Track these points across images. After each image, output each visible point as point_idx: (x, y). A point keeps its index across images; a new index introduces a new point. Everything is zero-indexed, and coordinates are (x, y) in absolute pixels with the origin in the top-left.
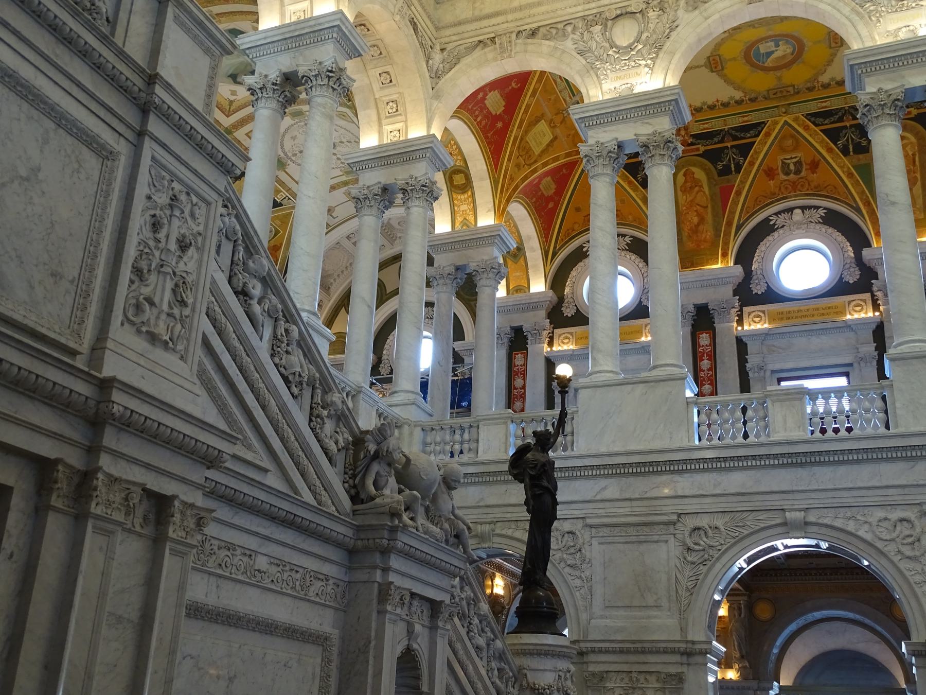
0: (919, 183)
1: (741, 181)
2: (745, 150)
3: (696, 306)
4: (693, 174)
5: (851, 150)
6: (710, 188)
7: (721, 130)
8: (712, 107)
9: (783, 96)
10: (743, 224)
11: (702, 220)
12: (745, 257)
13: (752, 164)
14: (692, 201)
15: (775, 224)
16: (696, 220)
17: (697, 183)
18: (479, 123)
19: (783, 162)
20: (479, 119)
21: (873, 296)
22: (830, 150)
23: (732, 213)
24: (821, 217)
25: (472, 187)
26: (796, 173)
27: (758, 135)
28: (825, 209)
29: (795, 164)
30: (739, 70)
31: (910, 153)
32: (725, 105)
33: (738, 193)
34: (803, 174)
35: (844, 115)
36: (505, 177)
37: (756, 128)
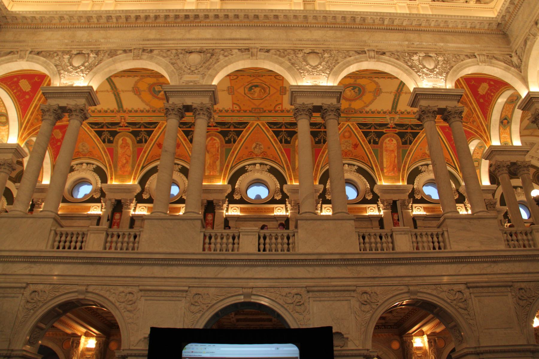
0: (219, 160)
2: (149, 133)
7: (140, 123)
8: (136, 111)
13: (152, 140)
16: (125, 161)
17: (127, 144)
18: (15, 93)
20: (15, 91)
22: (185, 140)
23: (141, 161)
25: (9, 124)
27: (155, 128)
30: (148, 96)
32: (142, 111)
33: (145, 152)
35: (191, 125)
36: (28, 123)
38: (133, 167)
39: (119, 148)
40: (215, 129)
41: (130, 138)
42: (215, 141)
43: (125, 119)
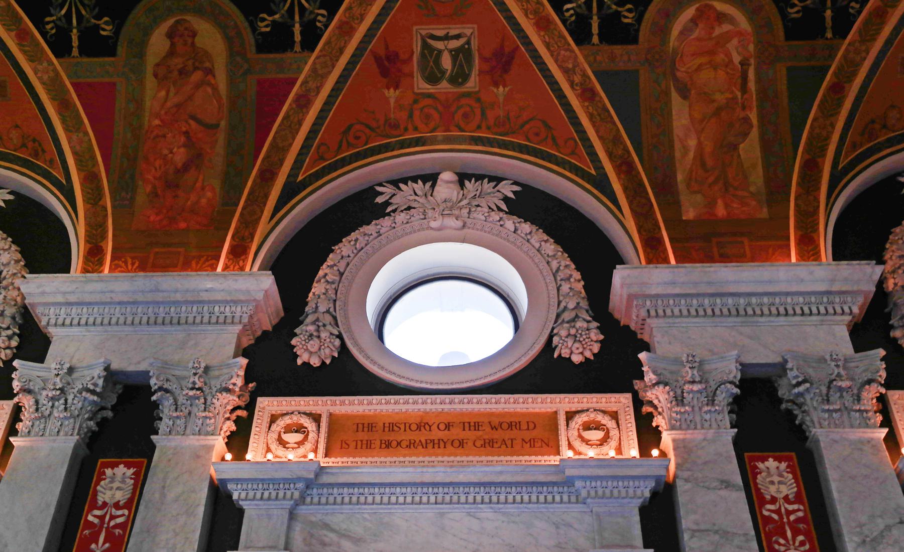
0: (755, 133)
1: (314, 70)
3: (111, 375)
4: (194, 35)
5: (595, 29)
6: (231, 82)
10: (304, 185)
11: (196, 160)
12: (295, 270)
13: (347, 30)
14: (178, 106)
15: (387, 203)
16: (180, 156)
17: (200, 61)
19: (425, 45)
21: (638, 403)
22: (543, 24)
23: (279, 150)
24: (506, 199)
26: (453, 80)
28: (516, 183)
29: (455, 54)
31: (737, 59)
33: (304, 102)
34: (472, 84)
39: (150, 82)
42: (726, 27)
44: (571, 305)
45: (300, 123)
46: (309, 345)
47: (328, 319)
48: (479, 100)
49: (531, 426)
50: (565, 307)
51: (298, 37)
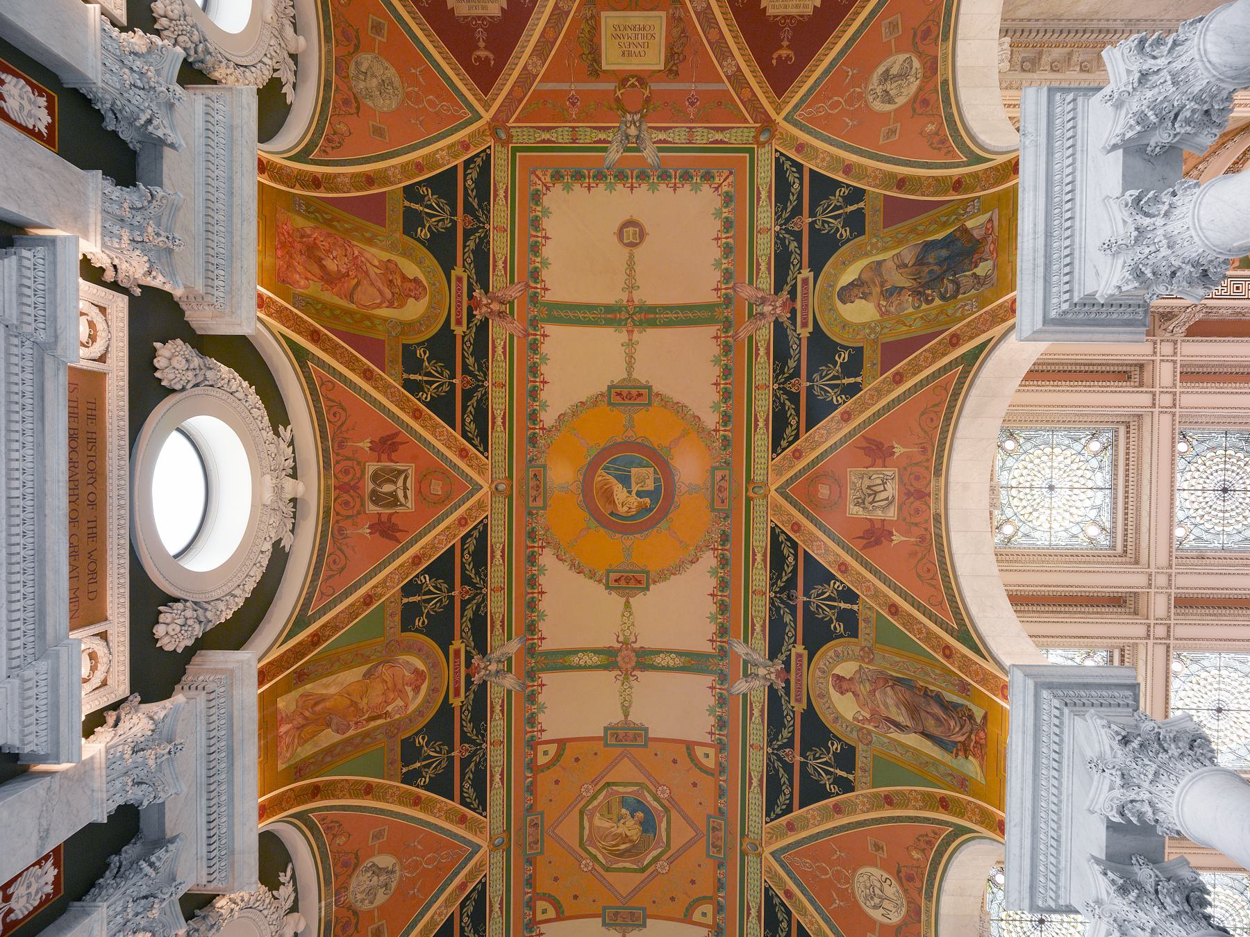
2: (443, 407)
4: (417, 299)
6: (385, 320)
7: (486, 375)
9: (529, 489)
10: (303, 365)
11: (330, 279)
13: (417, 414)
14: (367, 273)
16: (331, 265)
17: (398, 300)
19: (400, 472)
22: (416, 560)
23: (333, 350)
26: (374, 492)
27: (464, 435)
29: (393, 495)
31: (389, 708)
33: (367, 375)
34: (372, 508)
35: (473, 585)
37: (481, 438)
38: (307, 303)
39: (385, 256)
40: (457, 682)
41: (427, 318)
42: (411, 694)
43: (500, 314)
44: (209, 614)
45: (353, 370)
46: (179, 358)
47: (200, 379)
48: (359, 513)
49: (91, 596)
50: (206, 610)
51: (412, 377)
